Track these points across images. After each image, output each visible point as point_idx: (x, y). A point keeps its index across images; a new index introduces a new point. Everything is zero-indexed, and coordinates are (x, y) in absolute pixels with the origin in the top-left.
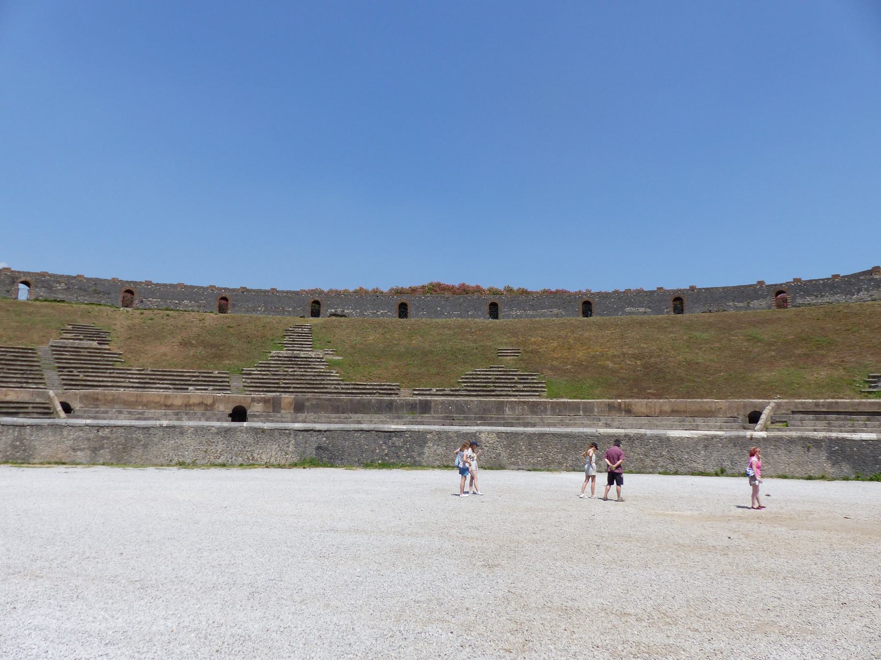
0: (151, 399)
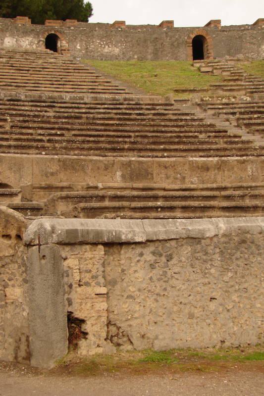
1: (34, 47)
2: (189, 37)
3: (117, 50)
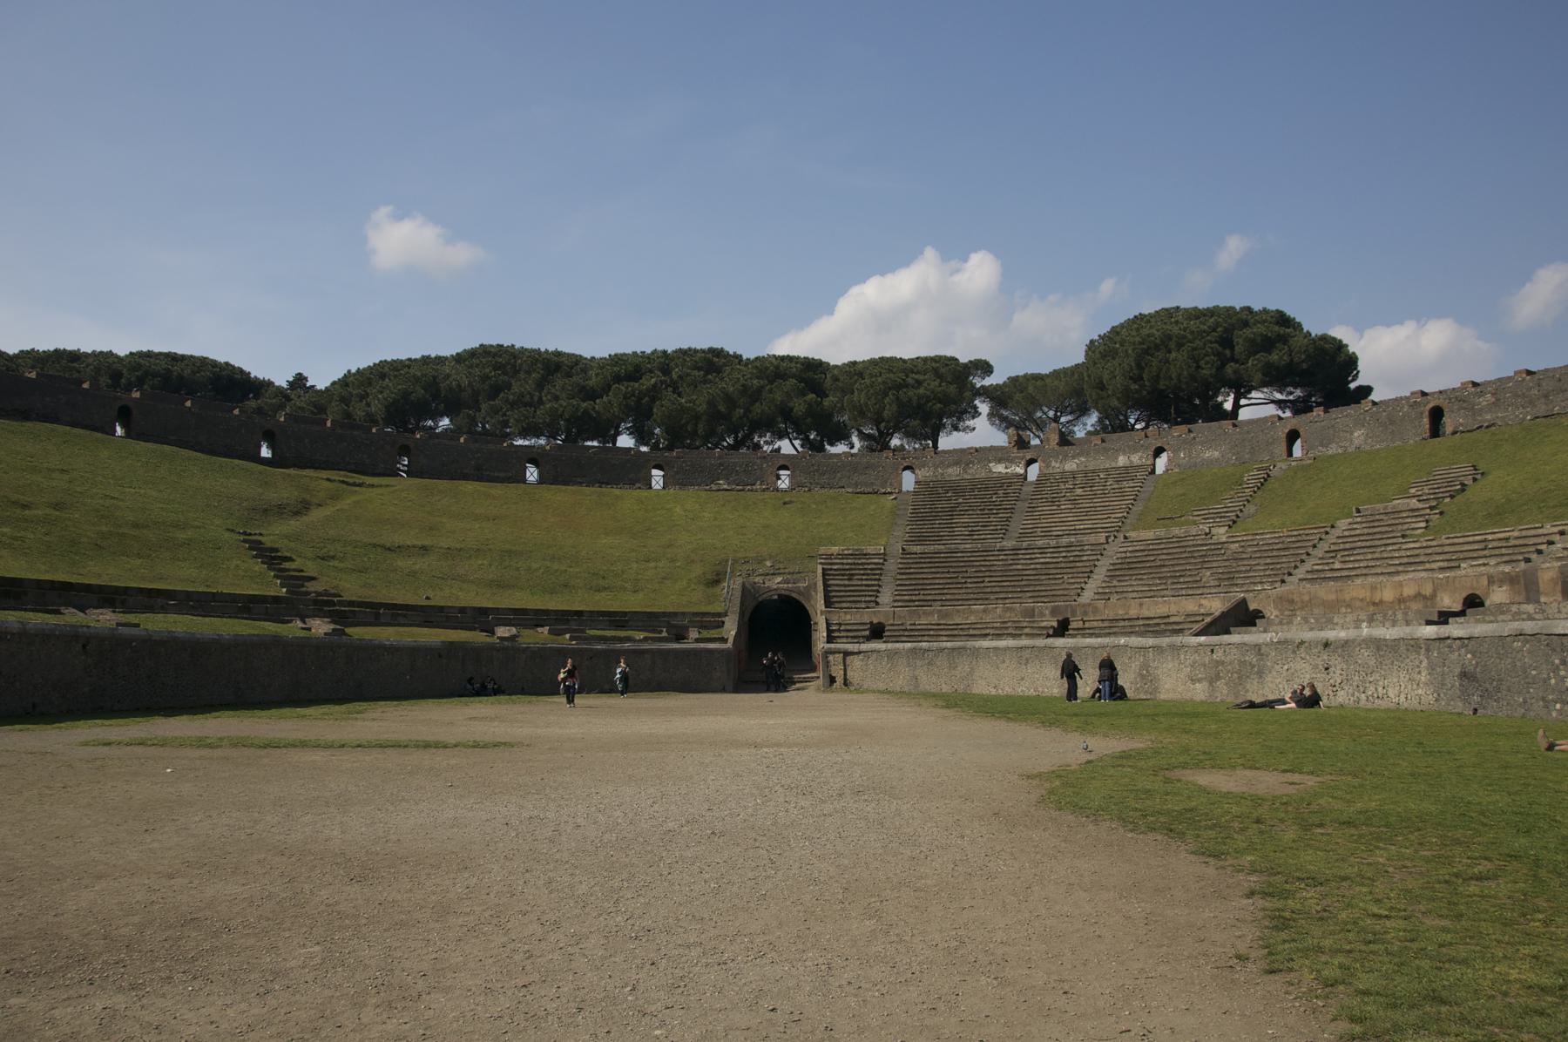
0: (1354, 594)
1: (1144, 460)
2: (1283, 433)
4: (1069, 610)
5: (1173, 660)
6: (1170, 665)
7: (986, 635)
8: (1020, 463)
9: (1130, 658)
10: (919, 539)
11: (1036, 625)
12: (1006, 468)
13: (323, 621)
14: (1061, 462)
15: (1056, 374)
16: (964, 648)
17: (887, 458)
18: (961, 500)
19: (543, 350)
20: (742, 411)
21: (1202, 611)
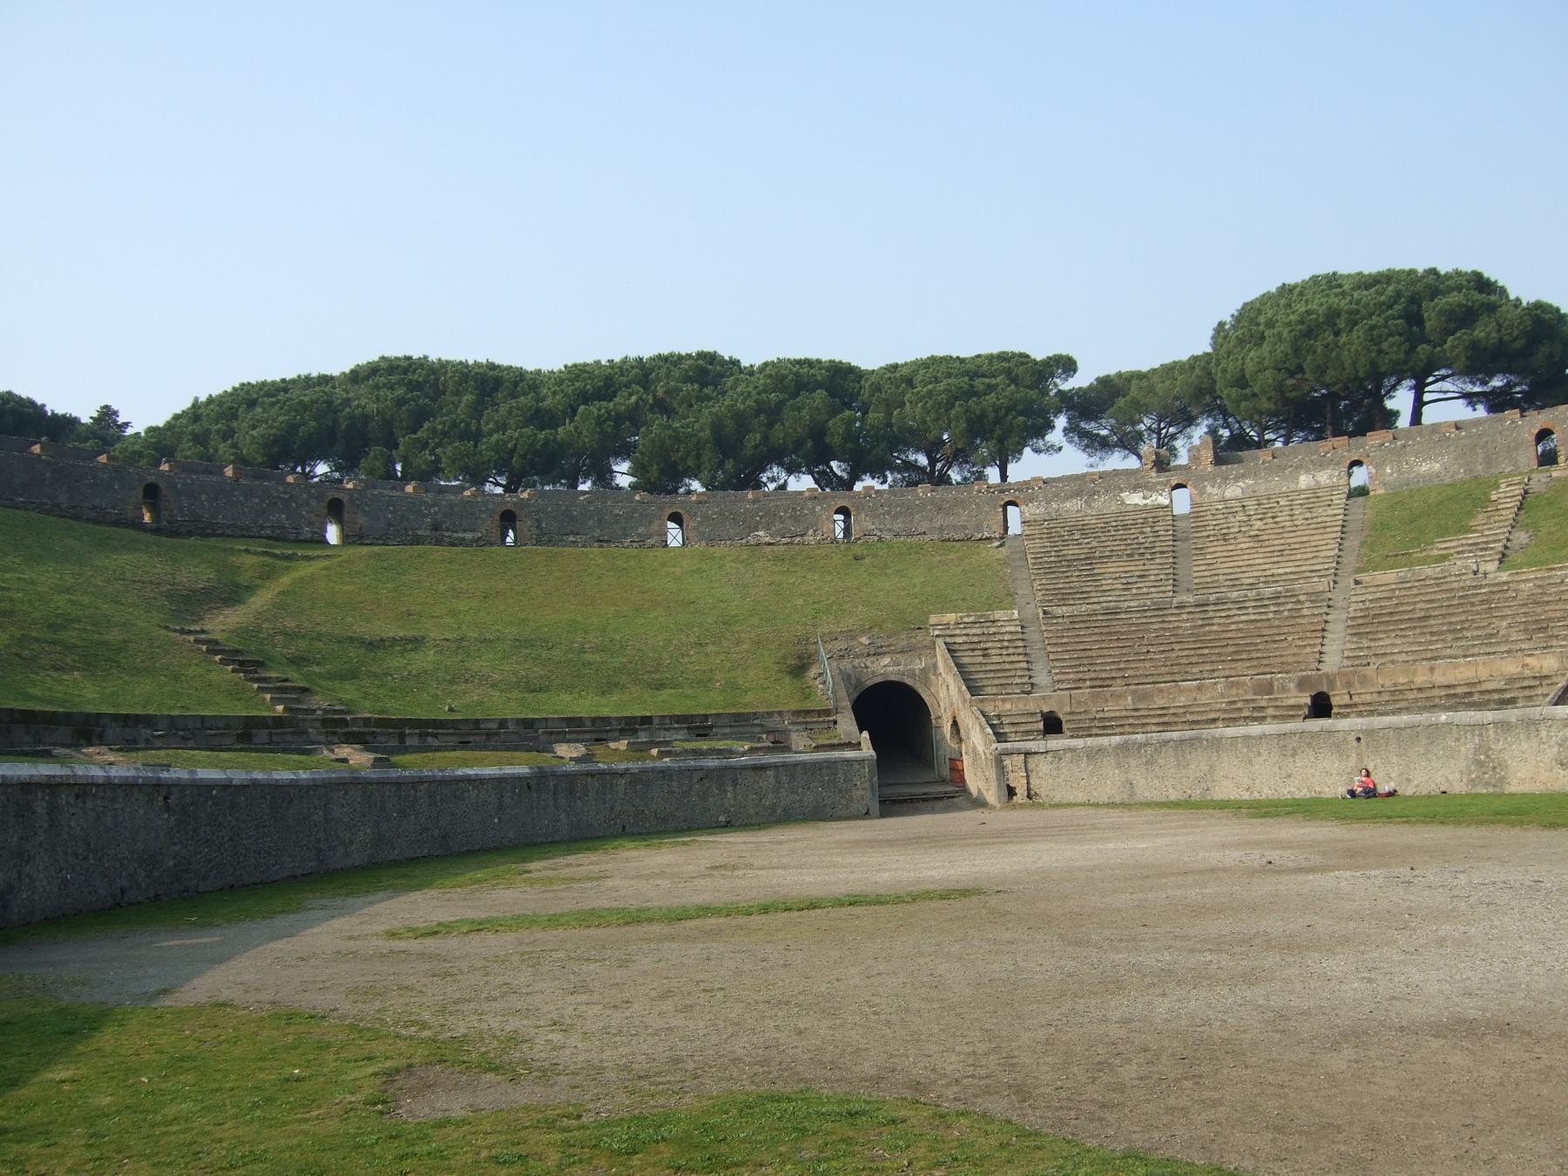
1: (1335, 480)
2: (1531, 433)
3: (1437, 466)
4: (1324, 680)
5: (1528, 738)
6: (1525, 746)
7: (1214, 720)
8: (1163, 490)
9: (1458, 740)
10: (1064, 598)
11: (1279, 704)
12: (1145, 498)
13: (354, 749)
14: (1220, 487)
15: (1170, 370)
16: (1198, 739)
17: (979, 491)
18: (1094, 544)
19: (471, 362)
20: (758, 436)
21: (1527, 672)
